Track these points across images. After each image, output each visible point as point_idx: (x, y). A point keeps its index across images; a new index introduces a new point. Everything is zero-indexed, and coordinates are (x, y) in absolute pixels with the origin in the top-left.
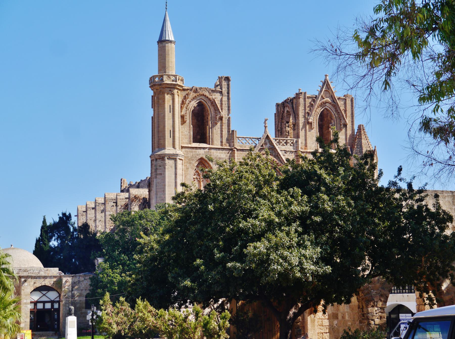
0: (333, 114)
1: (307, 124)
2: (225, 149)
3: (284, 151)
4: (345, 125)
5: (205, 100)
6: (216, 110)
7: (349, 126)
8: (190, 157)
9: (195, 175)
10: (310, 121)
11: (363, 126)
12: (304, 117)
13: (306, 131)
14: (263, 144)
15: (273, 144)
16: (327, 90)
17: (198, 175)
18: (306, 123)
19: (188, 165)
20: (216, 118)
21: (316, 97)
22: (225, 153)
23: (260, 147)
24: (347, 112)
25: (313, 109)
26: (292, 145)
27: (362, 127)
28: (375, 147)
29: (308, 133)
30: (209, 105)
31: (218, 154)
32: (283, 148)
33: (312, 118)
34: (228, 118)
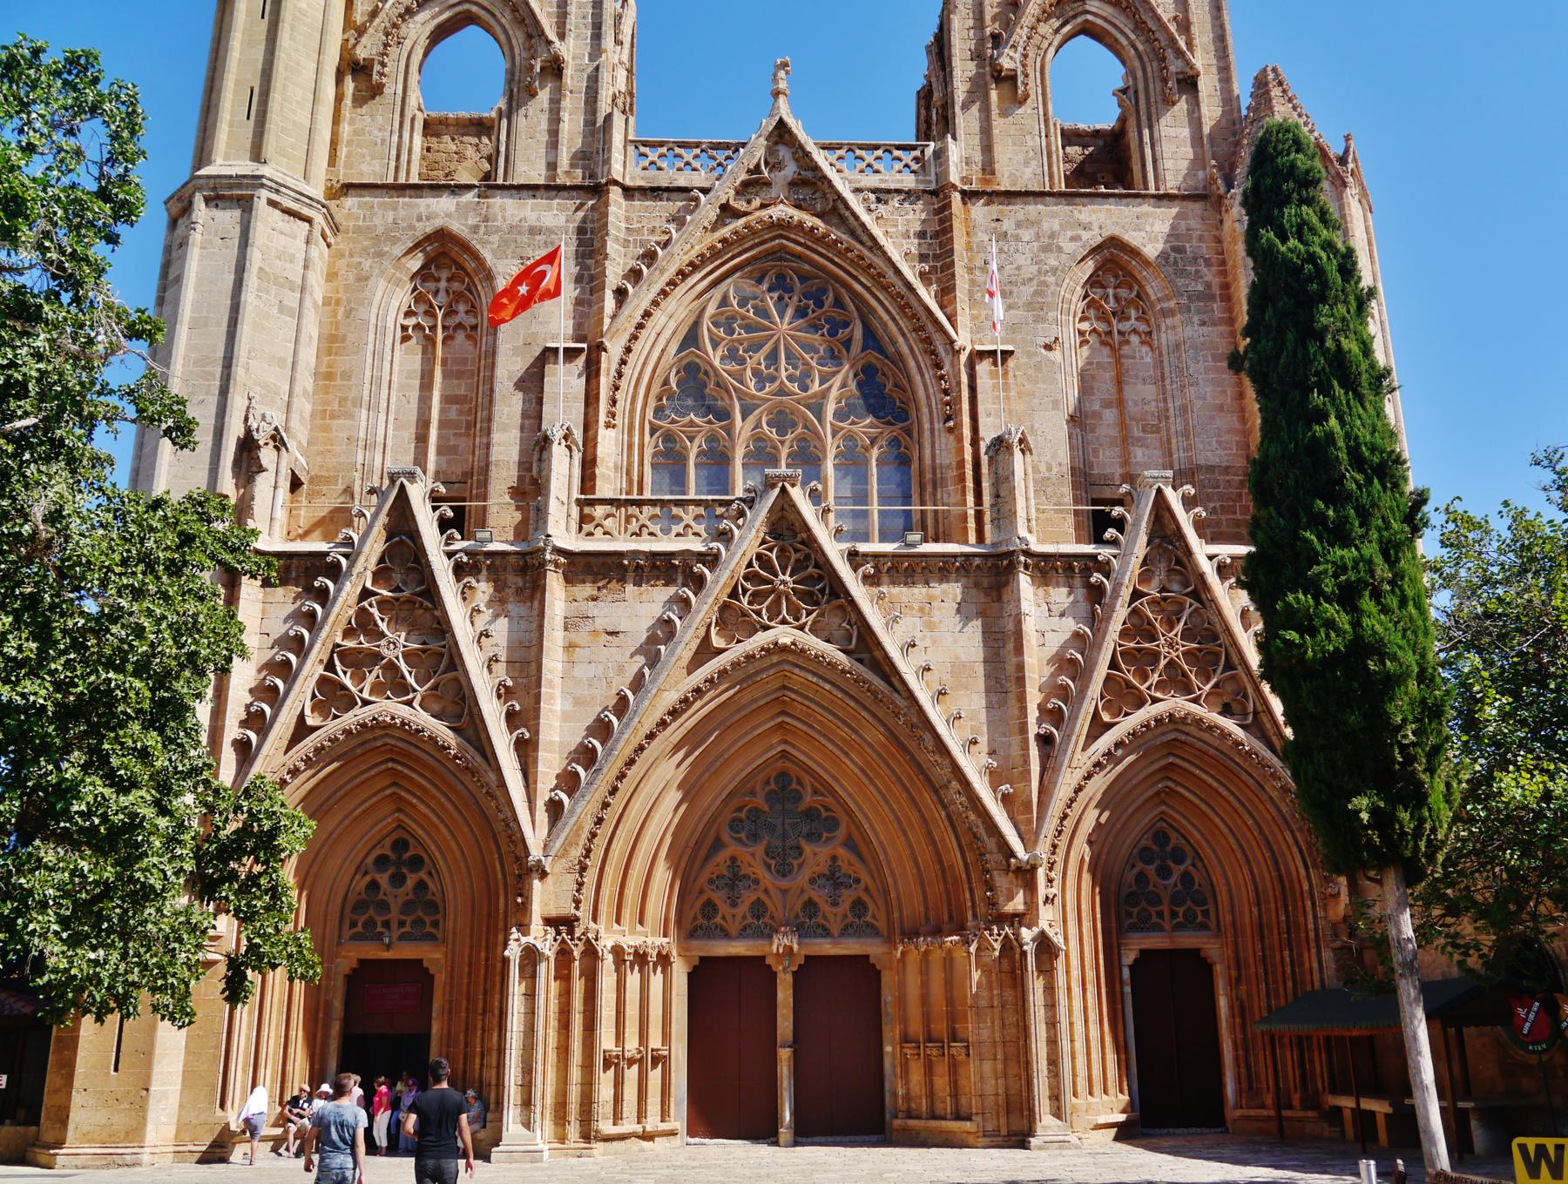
0: (1124, 41)
2: (563, 188)
3: (874, 191)
4: (1189, 83)
6: (530, 37)
7: (1207, 85)
8: (380, 230)
9: (409, 314)
10: (1006, 63)
11: (1274, 70)
12: (977, 55)
13: (986, 110)
14: (758, 166)
15: (812, 160)
17: (426, 313)
18: (988, 77)
19: (367, 264)
20: (532, 67)
22: (561, 209)
23: (743, 176)
24: (1195, 30)
25: (1018, 19)
26: (915, 166)
27: (1271, 76)
29: (998, 123)
30: (503, 21)
32: (871, 181)
33: (1017, 56)
34: (590, 69)
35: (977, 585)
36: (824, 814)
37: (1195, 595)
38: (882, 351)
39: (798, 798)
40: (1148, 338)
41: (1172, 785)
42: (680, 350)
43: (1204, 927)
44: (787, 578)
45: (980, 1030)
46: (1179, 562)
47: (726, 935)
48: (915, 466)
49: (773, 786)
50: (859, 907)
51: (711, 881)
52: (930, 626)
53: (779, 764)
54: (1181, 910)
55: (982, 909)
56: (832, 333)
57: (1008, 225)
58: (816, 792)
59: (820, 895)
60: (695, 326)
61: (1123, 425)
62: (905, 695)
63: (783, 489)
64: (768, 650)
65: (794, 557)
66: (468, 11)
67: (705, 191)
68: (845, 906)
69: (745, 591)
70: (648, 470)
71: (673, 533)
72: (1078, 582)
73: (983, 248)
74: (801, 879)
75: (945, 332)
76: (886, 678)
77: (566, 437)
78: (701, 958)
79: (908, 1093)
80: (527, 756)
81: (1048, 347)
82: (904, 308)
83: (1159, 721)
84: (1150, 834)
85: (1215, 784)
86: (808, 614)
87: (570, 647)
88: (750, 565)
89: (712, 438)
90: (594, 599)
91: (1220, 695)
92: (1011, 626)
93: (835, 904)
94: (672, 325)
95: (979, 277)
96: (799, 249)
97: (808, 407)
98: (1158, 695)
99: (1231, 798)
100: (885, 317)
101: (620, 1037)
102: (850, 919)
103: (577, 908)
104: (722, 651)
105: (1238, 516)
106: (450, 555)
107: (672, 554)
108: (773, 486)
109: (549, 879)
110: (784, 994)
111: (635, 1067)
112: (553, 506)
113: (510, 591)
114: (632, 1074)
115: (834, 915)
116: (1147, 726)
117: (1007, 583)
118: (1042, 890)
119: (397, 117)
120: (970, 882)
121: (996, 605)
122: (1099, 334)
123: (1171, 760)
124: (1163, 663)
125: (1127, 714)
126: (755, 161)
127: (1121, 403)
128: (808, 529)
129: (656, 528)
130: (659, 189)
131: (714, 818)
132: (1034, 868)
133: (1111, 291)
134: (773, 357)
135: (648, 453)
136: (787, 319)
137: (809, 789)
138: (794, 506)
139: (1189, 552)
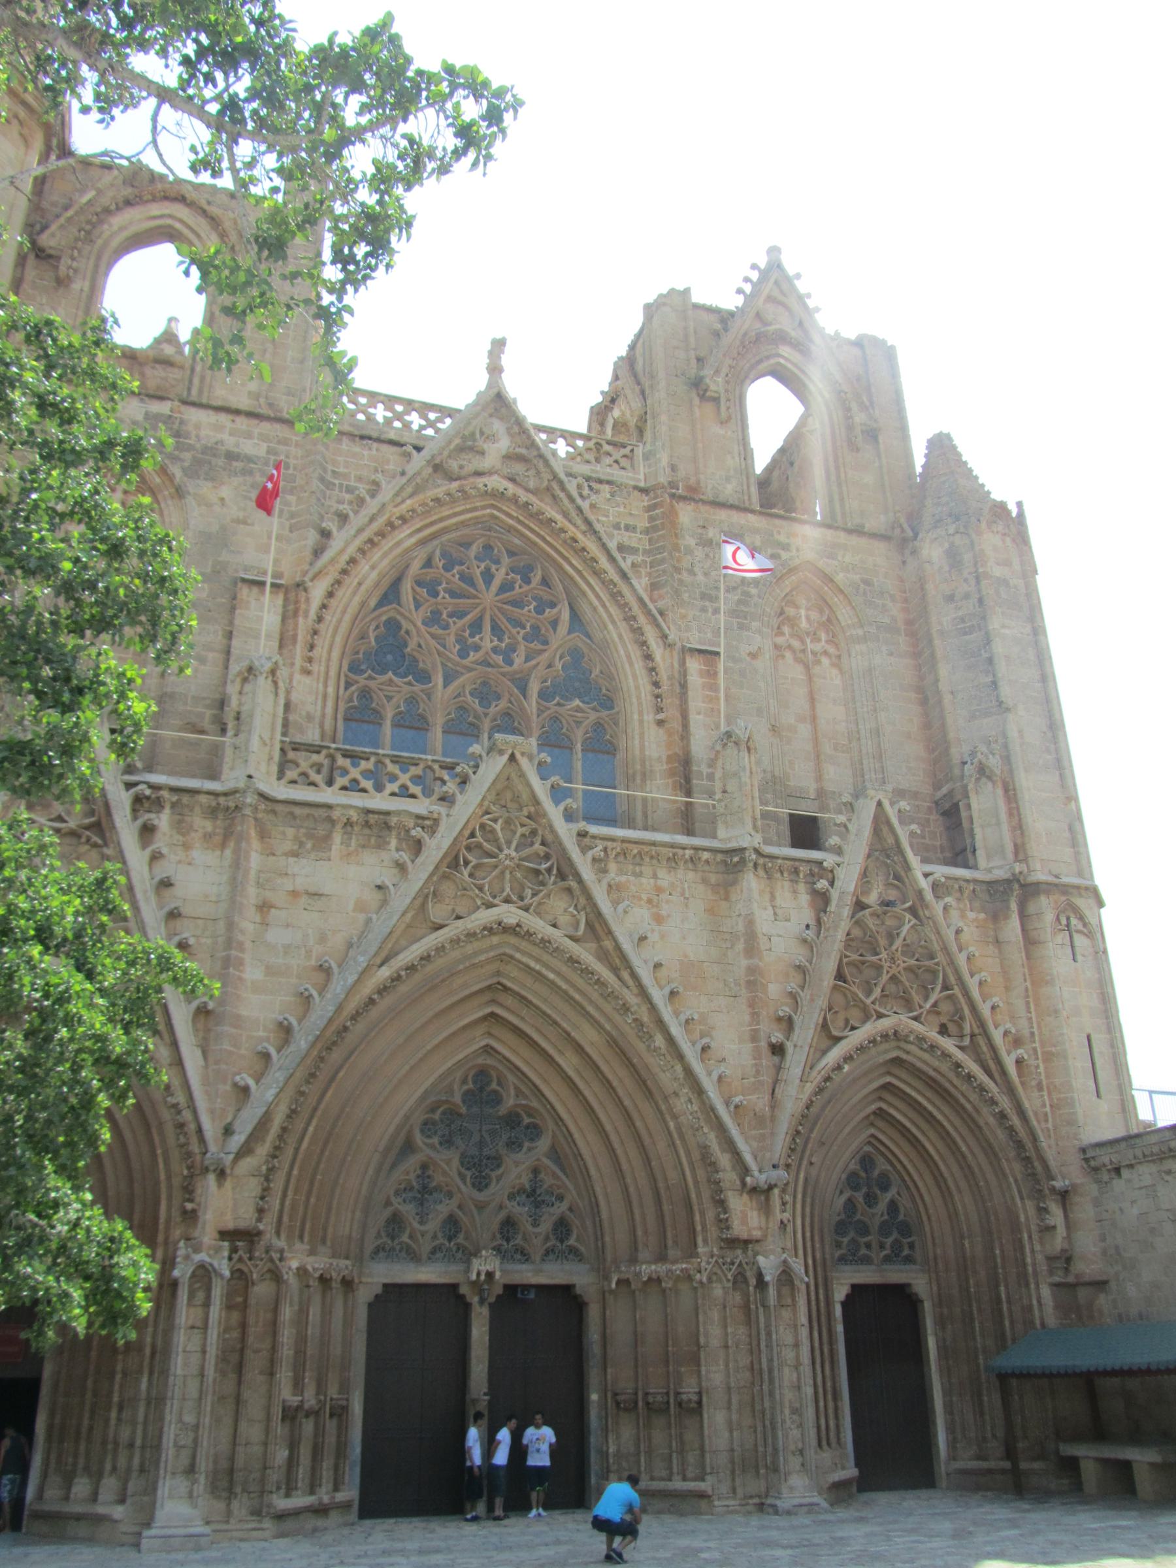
1: (696, 400)
3: (588, 479)
5: (191, 222)
14: (473, 434)
16: (780, 298)
21: (732, 314)
22: (264, 438)
28: (1019, 505)
31: (225, 437)
35: (705, 881)
36: (527, 1120)
37: (913, 911)
38: (588, 636)
39: (496, 1099)
40: (837, 663)
41: (884, 1106)
42: (380, 604)
43: (909, 1260)
44: (514, 854)
45: (715, 1375)
46: (897, 877)
47: (413, 1257)
48: (620, 755)
49: (471, 1086)
50: (562, 1228)
51: (397, 1193)
52: (658, 919)
53: (480, 1061)
54: (845, 1240)
55: (713, 1232)
56: (540, 610)
57: (711, 533)
58: (519, 1093)
59: (520, 1211)
60: (396, 583)
61: (816, 741)
62: (635, 991)
63: (512, 758)
64: (490, 930)
65: (520, 831)
66: (170, 226)
67: (418, 449)
68: (546, 1226)
69: (466, 863)
70: (340, 723)
71: (388, 791)
72: (802, 887)
73: (689, 551)
74: (497, 1191)
75: (658, 626)
76: (615, 970)
77: (273, 672)
78: (385, 1286)
79: (618, 1451)
80: (208, 1030)
81: (753, 656)
82: (616, 596)
83: (885, 1037)
84: (858, 1157)
85: (930, 1107)
86: (534, 895)
87: (264, 907)
88: (472, 835)
89: (412, 700)
90: (295, 854)
91: (938, 1013)
92: (741, 927)
93: (535, 1224)
94: (374, 575)
95: (685, 576)
96: (511, 522)
97: (513, 681)
98: (882, 1011)
99: (945, 1123)
100: (596, 603)
101: (298, 1385)
102: (441, 1240)
103: (259, 1220)
104: (441, 927)
105: (927, 841)
106: (129, 786)
107: (388, 813)
108: (501, 752)
109: (228, 1184)
110: (480, 1332)
111: (311, 1420)
112: (255, 743)
113: (196, 836)
114: (308, 1427)
115: (538, 1233)
116: (873, 1041)
117: (734, 883)
118: (778, 1215)
119: (81, 313)
120: (700, 1203)
121: (724, 904)
122: (794, 651)
123: (888, 1079)
124: (885, 978)
125: (853, 1028)
126: (471, 428)
127: (814, 719)
128: (536, 802)
129: (367, 784)
130: (370, 438)
131: (407, 1118)
132: (771, 1187)
133: (803, 612)
134: (477, 626)
135: (342, 706)
136: (494, 588)
137: (512, 1092)
138: (522, 775)
139: (908, 867)
